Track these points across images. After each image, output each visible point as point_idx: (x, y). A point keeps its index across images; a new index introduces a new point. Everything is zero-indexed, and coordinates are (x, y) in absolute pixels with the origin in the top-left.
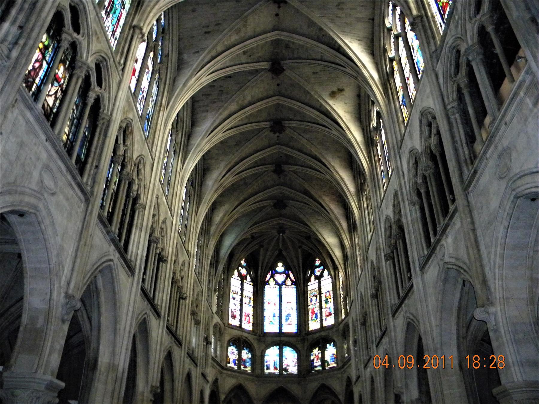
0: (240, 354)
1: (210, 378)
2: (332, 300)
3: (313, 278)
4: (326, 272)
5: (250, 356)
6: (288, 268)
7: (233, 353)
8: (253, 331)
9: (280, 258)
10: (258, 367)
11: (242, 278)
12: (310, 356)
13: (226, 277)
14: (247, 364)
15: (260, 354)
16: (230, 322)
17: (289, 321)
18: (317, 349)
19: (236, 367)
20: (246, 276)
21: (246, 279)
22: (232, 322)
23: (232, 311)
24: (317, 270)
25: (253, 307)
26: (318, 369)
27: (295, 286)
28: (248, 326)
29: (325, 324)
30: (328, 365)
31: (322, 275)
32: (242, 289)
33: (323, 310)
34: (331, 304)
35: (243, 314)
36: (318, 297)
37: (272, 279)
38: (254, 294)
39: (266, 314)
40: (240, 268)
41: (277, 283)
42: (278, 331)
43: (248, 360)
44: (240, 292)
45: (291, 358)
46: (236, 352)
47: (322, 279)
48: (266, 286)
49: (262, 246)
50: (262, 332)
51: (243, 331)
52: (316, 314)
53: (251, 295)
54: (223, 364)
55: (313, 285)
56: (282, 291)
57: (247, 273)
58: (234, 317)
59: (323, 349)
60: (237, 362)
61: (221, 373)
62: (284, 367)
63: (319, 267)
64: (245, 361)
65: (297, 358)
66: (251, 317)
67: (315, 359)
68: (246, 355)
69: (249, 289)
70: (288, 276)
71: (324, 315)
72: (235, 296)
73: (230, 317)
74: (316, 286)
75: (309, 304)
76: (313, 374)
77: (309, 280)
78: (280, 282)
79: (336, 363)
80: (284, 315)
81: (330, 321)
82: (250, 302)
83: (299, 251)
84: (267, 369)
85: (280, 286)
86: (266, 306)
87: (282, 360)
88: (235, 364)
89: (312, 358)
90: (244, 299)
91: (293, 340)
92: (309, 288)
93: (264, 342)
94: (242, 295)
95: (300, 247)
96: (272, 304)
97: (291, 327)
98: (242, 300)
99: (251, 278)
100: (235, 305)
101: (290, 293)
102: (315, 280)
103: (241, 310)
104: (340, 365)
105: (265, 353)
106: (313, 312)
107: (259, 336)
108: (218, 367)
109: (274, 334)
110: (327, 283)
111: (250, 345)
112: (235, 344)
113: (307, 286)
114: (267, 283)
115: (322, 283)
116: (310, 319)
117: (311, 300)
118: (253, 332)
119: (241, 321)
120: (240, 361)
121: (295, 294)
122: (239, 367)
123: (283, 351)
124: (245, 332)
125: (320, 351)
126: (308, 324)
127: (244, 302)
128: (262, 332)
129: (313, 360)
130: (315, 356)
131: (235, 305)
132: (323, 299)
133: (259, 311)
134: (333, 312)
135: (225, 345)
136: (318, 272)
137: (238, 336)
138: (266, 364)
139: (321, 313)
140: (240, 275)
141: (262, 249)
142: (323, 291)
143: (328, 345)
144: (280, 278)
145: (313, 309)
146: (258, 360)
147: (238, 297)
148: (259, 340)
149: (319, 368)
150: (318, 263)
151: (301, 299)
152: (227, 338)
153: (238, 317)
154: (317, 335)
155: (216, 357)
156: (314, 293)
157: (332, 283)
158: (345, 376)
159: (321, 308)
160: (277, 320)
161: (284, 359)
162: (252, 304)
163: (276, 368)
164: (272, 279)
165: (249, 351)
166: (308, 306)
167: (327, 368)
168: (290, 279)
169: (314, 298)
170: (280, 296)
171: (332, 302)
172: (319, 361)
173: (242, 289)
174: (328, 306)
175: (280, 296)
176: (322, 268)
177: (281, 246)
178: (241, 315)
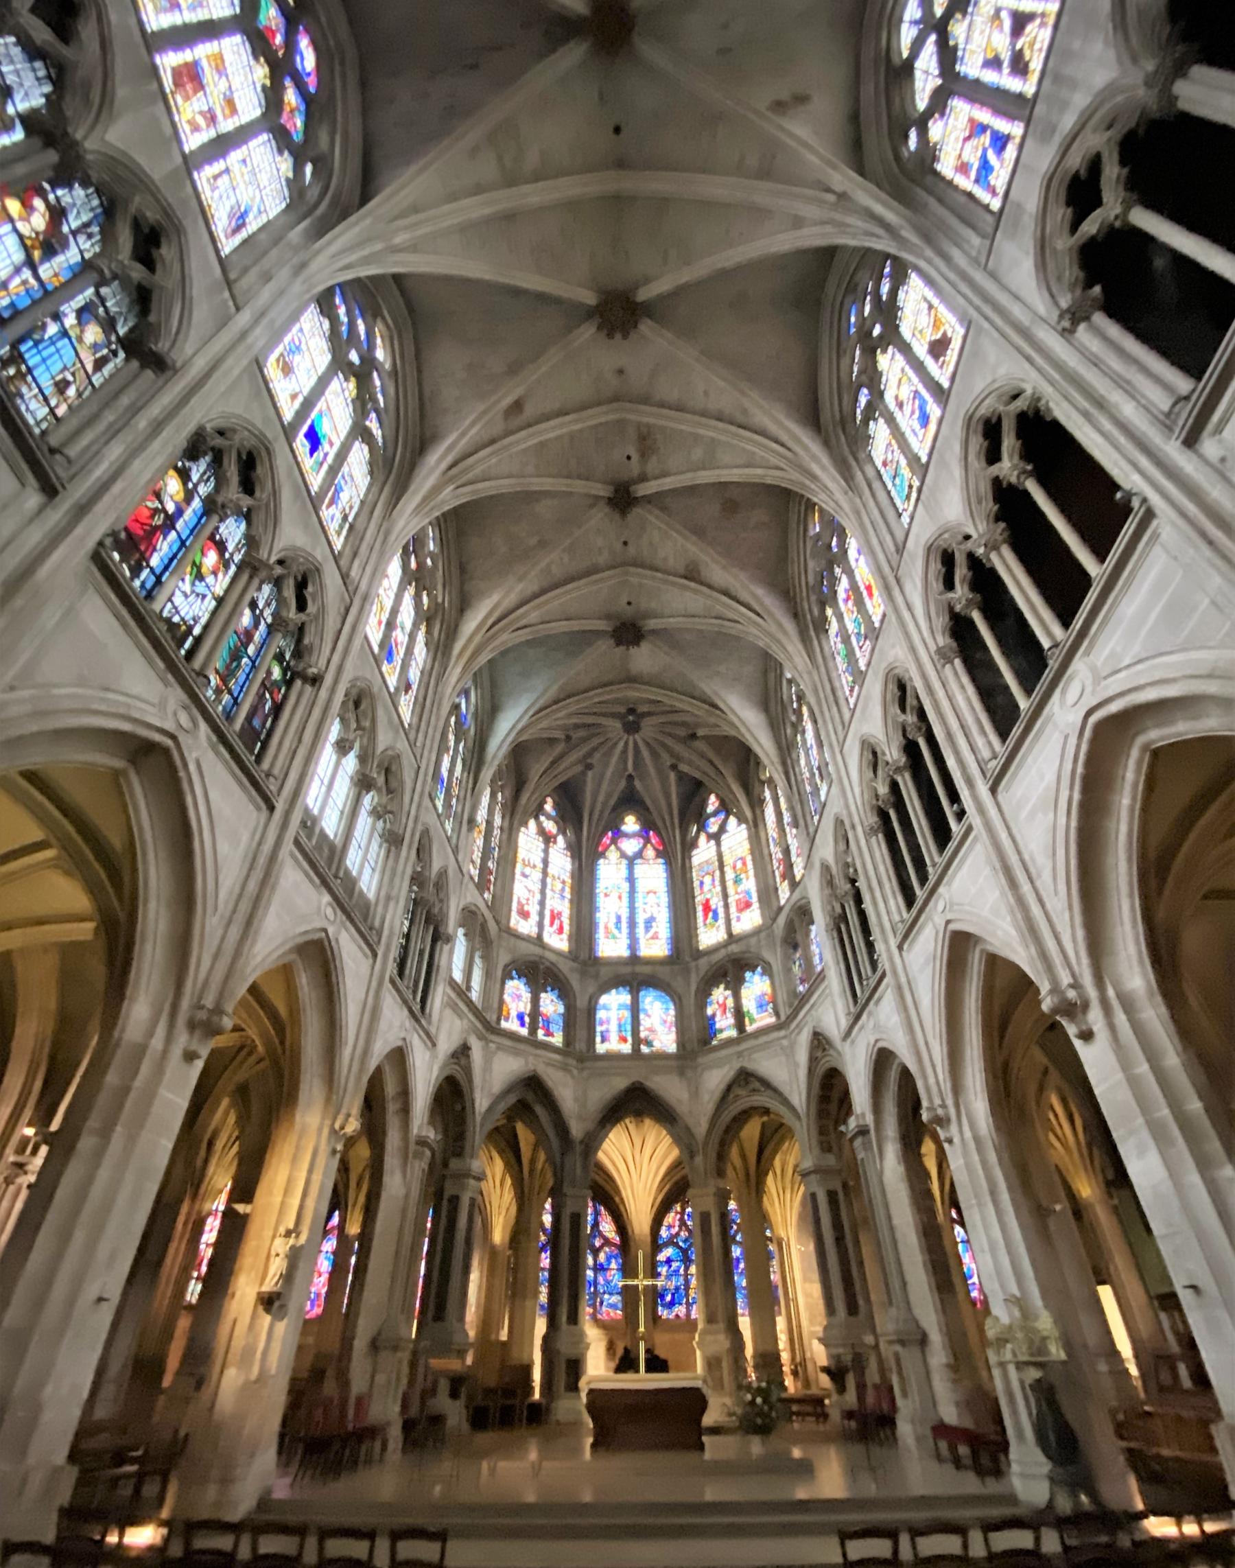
0: (535, 1001)
1: (446, 1045)
3: (703, 837)
4: (732, 820)
5: (561, 1009)
6: (648, 826)
7: (519, 997)
9: (630, 801)
10: (581, 1034)
11: (548, 839)
13: (506, 824)
14: (553, 1028)
15: (585, 1003)
18: (722, 986)
19: (524, 1032)
20: (555, 837)
22: (516, 922)
24: (712, 820)
25: (571, 901)
27: (661, 861)
28: (559, 942)
29: (739, 928)
30: (752, 1021)
31: (722, 829)
32: (546, 862)
34: (750, 884)
36: (717, 873)
40: (542, 818)
41: (623, 855)
48: (601, 861)
49: (589, 767)
54: (491, 1017)
55: (703, 853)
58: (525, 915)
59: (736, 986)
60: (527, 1019)
61: (481, 1038)
62: (643, 1035)
63: (715, 814)
64: (548, 1021)
67: (719, 1014)
68: (551, 1004)
69: (561, 862)
70: (647, 841)
71: (733, 909)
72: (528, 871)
76: (716, 1048)
77: (694, 844)
78: (630, 852)
79: (777, 1014)
80: (641, 919)
81: (749, 921)
82: (563, 890)
83: (672, 776)
84: (603, 1041)
85: (631, 861)
86: (601, 901)
88: (523, 1025)
89: (709, 1011)
90: (549, 880)
91: (663, 973)
93: (596, 976)
94: (545, 873)
95: (674, 767)
96: (614, 895)
97: (656, 946)
101: (653, 874)
103: (542, 903)
104: (783, 1018)
106: (707, 907)
107: (584, 963)
108: (470, 1016)
113: (690, 858)
114: (602, 855)
117: (702, 883)
118: (573, 956)
119: (540, 925)
122: (533, 1030)
125: (728, 993)
132: (730, 875)
133: (585, 910)
135: (499, 973)
136: (713, 827)
138: (599, 1029)
139: (726, 906)
140: (542, 832)
141: (590, 774)
142: (728, 860)
144: (631, 846)
145: (708, 901)
146: (580, 1021)
147: (537, 875)
148: (583, 974)
149: (733, 1033)
150: (713, 803)
152: (503, 958)
153: (534, 918)
154: (723, 953)
155: (469, 988)
157: (750, 838)
158: (804, 1038)
159: (725, 896)
161: (642, 1016)
162: (568, 895)
163: (624, 1040)
165: (560, 997)
166: (694, 897)
167: (750, 1028)
170: (631, 879)
172: (729, 1015)
173: (546, 862)
174: (741, 888)
175: (631, 879)
176: (722, 816)
178: (541, 914)
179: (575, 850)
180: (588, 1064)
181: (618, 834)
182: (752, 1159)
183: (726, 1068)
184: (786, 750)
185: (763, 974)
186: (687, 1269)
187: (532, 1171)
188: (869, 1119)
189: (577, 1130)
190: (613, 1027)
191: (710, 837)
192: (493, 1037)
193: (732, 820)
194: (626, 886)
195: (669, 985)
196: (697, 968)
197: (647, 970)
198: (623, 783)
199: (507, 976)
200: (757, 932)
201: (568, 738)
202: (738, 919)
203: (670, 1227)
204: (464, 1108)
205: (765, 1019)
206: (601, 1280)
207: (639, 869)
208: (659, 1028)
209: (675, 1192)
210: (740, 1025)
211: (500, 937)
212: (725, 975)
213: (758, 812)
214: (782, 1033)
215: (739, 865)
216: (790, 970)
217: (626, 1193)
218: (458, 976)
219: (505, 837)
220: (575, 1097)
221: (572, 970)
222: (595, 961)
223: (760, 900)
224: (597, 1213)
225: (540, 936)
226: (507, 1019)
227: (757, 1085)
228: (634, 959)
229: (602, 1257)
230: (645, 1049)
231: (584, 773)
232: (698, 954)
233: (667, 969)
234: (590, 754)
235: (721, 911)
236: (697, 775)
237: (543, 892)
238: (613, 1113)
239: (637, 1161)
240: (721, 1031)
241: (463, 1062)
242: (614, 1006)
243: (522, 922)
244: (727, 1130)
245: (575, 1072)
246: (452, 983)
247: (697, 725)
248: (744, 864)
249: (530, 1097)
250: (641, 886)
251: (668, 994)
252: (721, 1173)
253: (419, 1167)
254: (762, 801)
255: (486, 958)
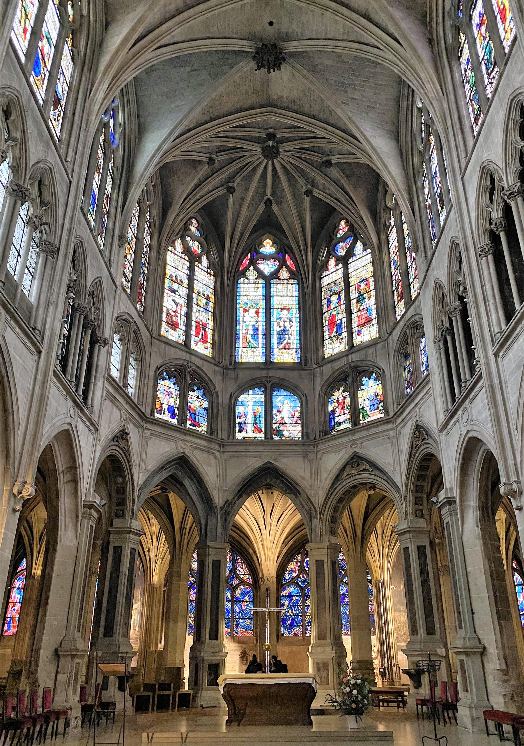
0: (184, 398)
1: (108, 429)
2: (373, 293)
3: (332, 262)
4: (359, 246)
5: (206, 405)
6: (283, 249)
7: (170, 394)
8: (213, 358)
9: (268, 225)
11: (193, 259)
12: (325, 405)
13: (155, 242)
14: (199, 419)
16: (163, 333)
17: (285, 342)
19: (174, 422)
20: (200, 257)
21: (200, 262)
22: (166, 332)
23: (168, 314)
24: (341, 244)
25: (214, 314)
26: (342, 427)
27: (296, 282)
29: (358, 340)
31: (350, 253)
32: (191, 278)
33: (353, 316)
34: (371, 302)
35: (194, 324)
37: (252, 268)
38: (215, 291)
39: (241, 329)
41: (261, 274)
42: (263, 360)
43: (202, 411)
44: (186, 282)
45: (287, 408)
46: (176, 393)
47: (351, 260)
48: (242, 280)
49: (231, 190)
50: (231, 360)
51: (191, 354)
52: (339, 326)
53: (210, 293)
55: (333, 275)
56: (272, 290)
57: (202, 251)
58: (174, 326)
60: (176, 412)
62: (274, 426)
63: (343, 239)
65: (299, 409)
66: (210, 333)
68: (197, 401)
69: (205, 281)
70: (283, 263)
71: (355, 325)
73: (164, 324)
74: (340, 273)
75: (325, 309)
77: (325, 267)
80: (275, 330)
81: (369, 334)
82: (207, 304)
83: (307, 201)
85: (268, 280)
86: (240, 313)
87: (271, 414)
91: (292, 376)
92: (325, 281)
93: (237, 378)
94: (190, 288)
95: (308, 193)
96: (252, 311)
97: (287, 355)
98: (190, 298)
99: (209, 262)
100: (177, 304)
101: (286, 295)
102: (337, 265)
103: (188, 316)
104: (391, 414)
105: (236, 400)
106: (332, 321)
107: (225, 368)
108: (127, 407)
109: (256, 366)
110: (362, 265)
111: (204, 381)
112: (175, 377)
115: (352, 267)
116: (326, 336)
117: (329, 302)
118: (215, 360)
120: (183, 410)
121: (297, 294)
122: (182, 422)
123: (274, 398)
124: (196, 356)
126: (323, 346)
127: (195, 301)
128: (231, 360)
129: (334, 411)
130: (337, 405)
131: (177, 304)
132: (354, 295)
133: (226, 322)
134: (374, 316)
135: (152, 374)
137: (181, 362)
138: (237, 421)
139: (349, 322)
140: (187, 251)
142: (353, 281)
143: (364, 379)
145: (333, 317)
147: (183, 291)
151: (309, 301)
152: (155, 361)
153: (182, 327)
154: (344, 360)
155: (126, 385)
156: (333, 289)
158: (408, 430)
159: (349, 312)
160: (261, 341)
161: (274, 412)
162: (211, 309)
163: (260, 431)
164: (252, 268)
166: (322, 314)
168: (287, 267)
169: (334, 298)
170: (268, 297)
171: (373, 298)
173: (191, 278)
175: (268, 297)
176: (350, 240)
177: (269, 195)
178: (188, 324)
179: (216, 270)
180: (229, 448)
181: (257, 256)
182: (359, 522)
183: (342, 453)
184: (413, 177)
185: (376, 380)
186: (304, 601)
187: (182, 529)
188: (456, 493)
189: (218, 499)
190: (250, 419)
191: (338, 260)
192: (148, 426)
193: (359, 246)
194: (262, 303)
195: (297, 387)
196: (322, 374)
197: (280, 374)
198: (261, 208)
199: (159, 376)
200: (373, 343)
201: (211, 161)
202: (359, 333)
203: (292, 571)
204: (124, 481)
205: (376, 415)
206: (237, 609)
207: (275, 289)
208: (287, 420)
209: (296, 546)
210: (355, 420)
211: (151, 343)
212: (345, 380)
213: (383, 237)
214: (390, 426)
215: (363, 286)
216: (400, 375)
217: (258, 547)
218: (115, 374)
219: (154, 254)
220: (217, 474)
221: (215, 373)
222: (236, 366)
223: (378, 317)
224: (234, 561)
225: (187, 344)
226: (160, 412)
227: (367, 466)
228: (268, 363)
229: (238, 592)
230: (276, 438)
231: (224, 200)
232: (323, 362)
233: (296, 373)
234: (231, 179)
235: (344, 325)
236: (329, 200)
237: (189, 306)
238: (248, 487)
239: (267, 525)
240: (340, 423)
241: (122, 444)
242: (251, 403)
243: (172, 331)
244: (340, 500)
245: (217, 454)
246: (110, 379)
247: (331, 153)
248: (367, 285)
249: (180, 474)
250: (276, 302)
251: (296, 394)
252: (333, 532)
253: (88, 524)
254: (387, 227)
255: (139, 360)
